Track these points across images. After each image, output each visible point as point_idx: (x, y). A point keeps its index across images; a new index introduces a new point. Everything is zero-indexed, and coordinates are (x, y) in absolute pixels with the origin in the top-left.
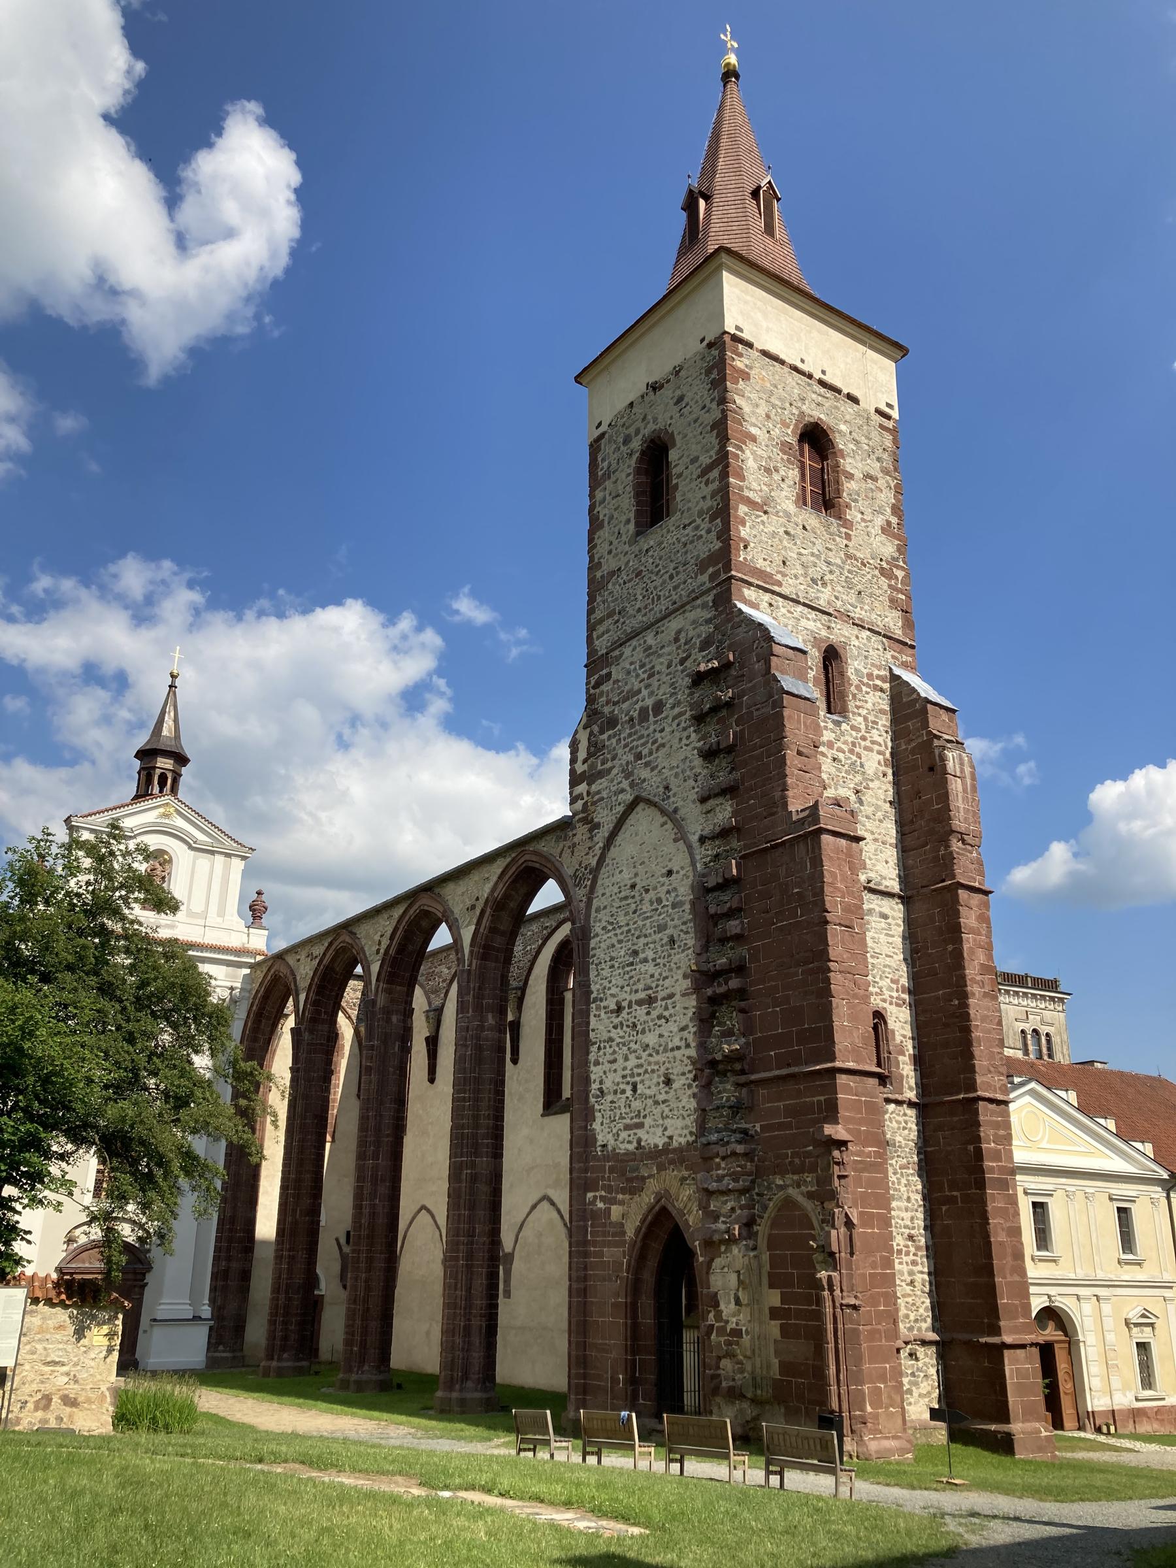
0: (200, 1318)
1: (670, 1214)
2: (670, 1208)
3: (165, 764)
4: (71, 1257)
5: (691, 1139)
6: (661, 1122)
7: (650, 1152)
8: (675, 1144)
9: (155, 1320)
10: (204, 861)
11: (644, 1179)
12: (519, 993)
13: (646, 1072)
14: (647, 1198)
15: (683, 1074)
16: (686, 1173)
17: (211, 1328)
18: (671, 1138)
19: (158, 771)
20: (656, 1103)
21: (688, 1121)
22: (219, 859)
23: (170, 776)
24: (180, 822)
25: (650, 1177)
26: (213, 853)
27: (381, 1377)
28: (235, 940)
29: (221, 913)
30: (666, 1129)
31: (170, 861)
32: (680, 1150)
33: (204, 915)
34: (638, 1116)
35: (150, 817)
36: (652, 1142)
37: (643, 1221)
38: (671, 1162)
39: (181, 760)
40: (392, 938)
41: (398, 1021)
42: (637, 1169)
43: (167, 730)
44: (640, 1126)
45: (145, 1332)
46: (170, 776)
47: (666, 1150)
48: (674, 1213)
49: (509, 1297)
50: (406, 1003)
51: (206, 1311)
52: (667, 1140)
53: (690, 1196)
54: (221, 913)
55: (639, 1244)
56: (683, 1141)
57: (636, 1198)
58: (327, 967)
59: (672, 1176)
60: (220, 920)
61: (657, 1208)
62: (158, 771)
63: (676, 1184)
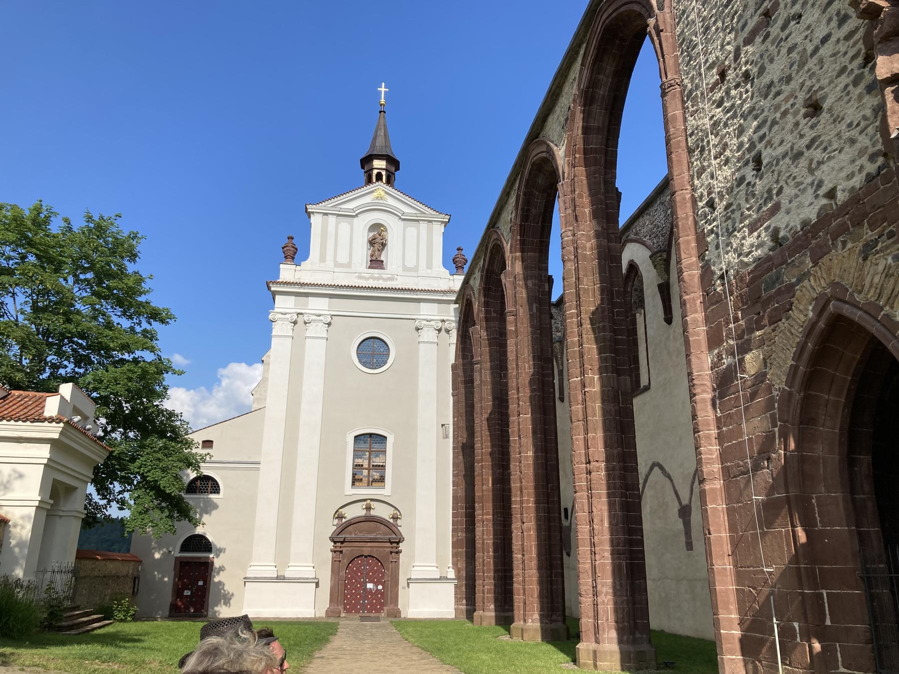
0: (447, 578)
1: (851, 322)
2: (847, 310)
3: (380, 164)
4: (340, 530)
5: (871, 168)
6: (809, 179)
7: (796, 239)
8: (841, 197)
9: (409, 579)
10: (412, 230)
11: (791, 288)
12: (665, 255)
13: (774, 123)
14: (803, 312)
15: (843, 70)
16: (868, 234)
17: (456, 587)
18: (831, 194)
19: (375, 172)
20: (800, 154)
21: (864, 141)
22: (423, 226)
23: (384, 173)
24: (391, 201)
25: (799, 281)
26: (418, 221)
27: (553, 626)
28: (444, 287)
29: (429, 266)
30: (820, 184)
31: (386, 230)
32: (855, 198)
33: (416, 269)
34: (770, 198)
35: (368, 199)
36: (795, 222)
37: (798, 356)
38: (843, 230)
39: (393, 162)
40: (517, 209)
41: (534, 285)
42: (778, 277)
43: (380, 142)
44: (776, 208)
45: (404, 588)
46: (384, 173)
47: (824, 218)
48: (857, 315)
49: (691, 549)
50: (540, 269)
51: (451, 574)
52: (824, 201)
53: (888, 267)
54: (429, 266)
55: (797, 397)
56: (857, 181)
57: (783, 324)
58: (487, 270)
59: (843, 261)
60: (429, 271)
61: (822, 324)
62: (375, 172)
63: (853, 262)
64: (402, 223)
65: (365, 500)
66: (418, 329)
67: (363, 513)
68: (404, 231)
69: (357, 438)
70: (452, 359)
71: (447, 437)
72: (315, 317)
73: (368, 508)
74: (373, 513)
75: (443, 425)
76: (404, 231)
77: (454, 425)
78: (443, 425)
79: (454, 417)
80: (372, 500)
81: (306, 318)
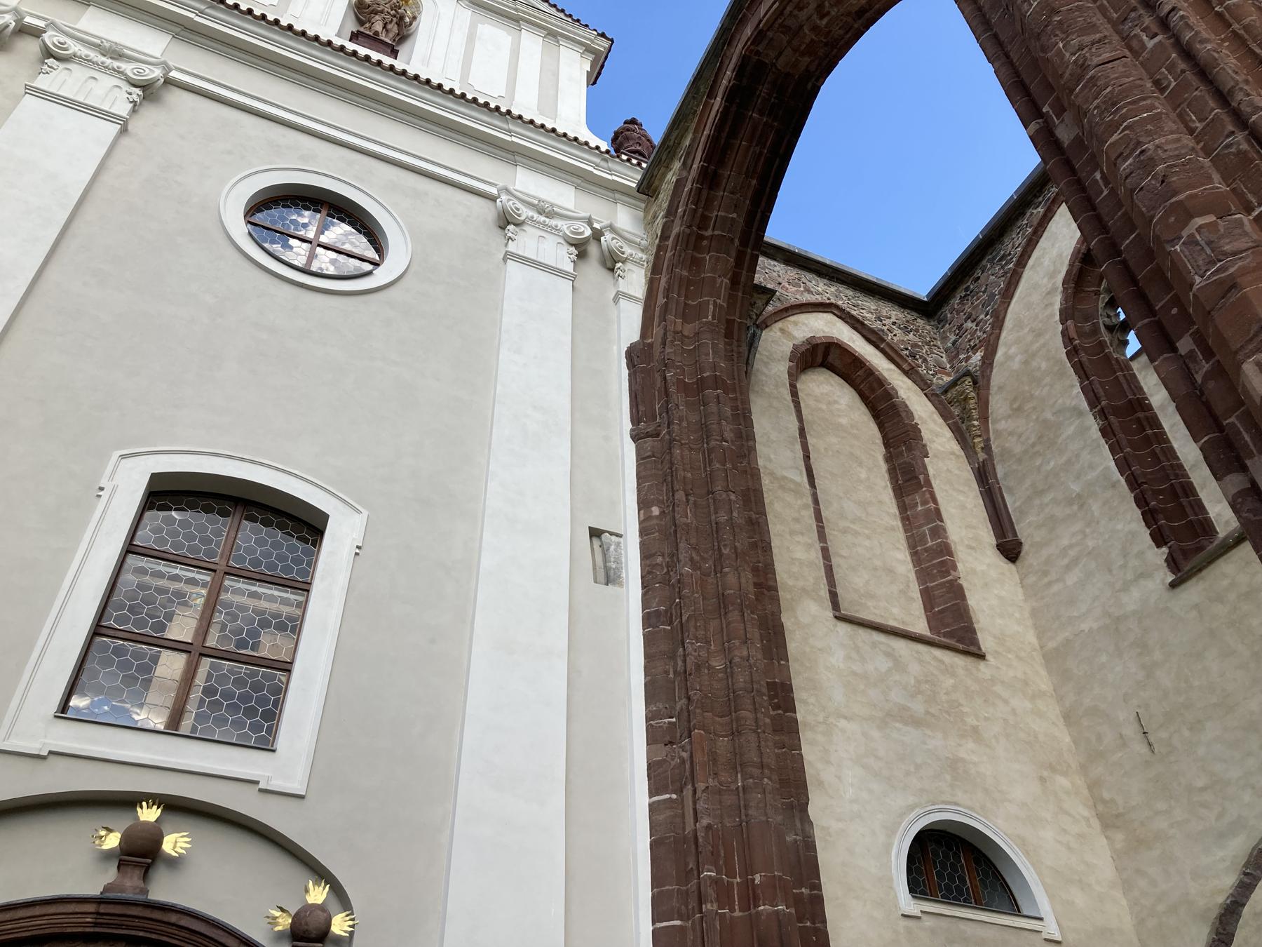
22: (532, 43)
64: (467, 14)
65: (128, 802)
66: (506, 221)
67: (88, 880)
68: (471, 38)
69: (165, 493)
70: (628, 324)
71: (610, 576)
72: (93, 55)
73: (141, 854)
74: (163, 890)
75: (595, 533)
76: (471, 38)
77: (643, 532)
78: (595, 533)
79: (643, 504)
80: (175, 807)
81: (50, 38)
